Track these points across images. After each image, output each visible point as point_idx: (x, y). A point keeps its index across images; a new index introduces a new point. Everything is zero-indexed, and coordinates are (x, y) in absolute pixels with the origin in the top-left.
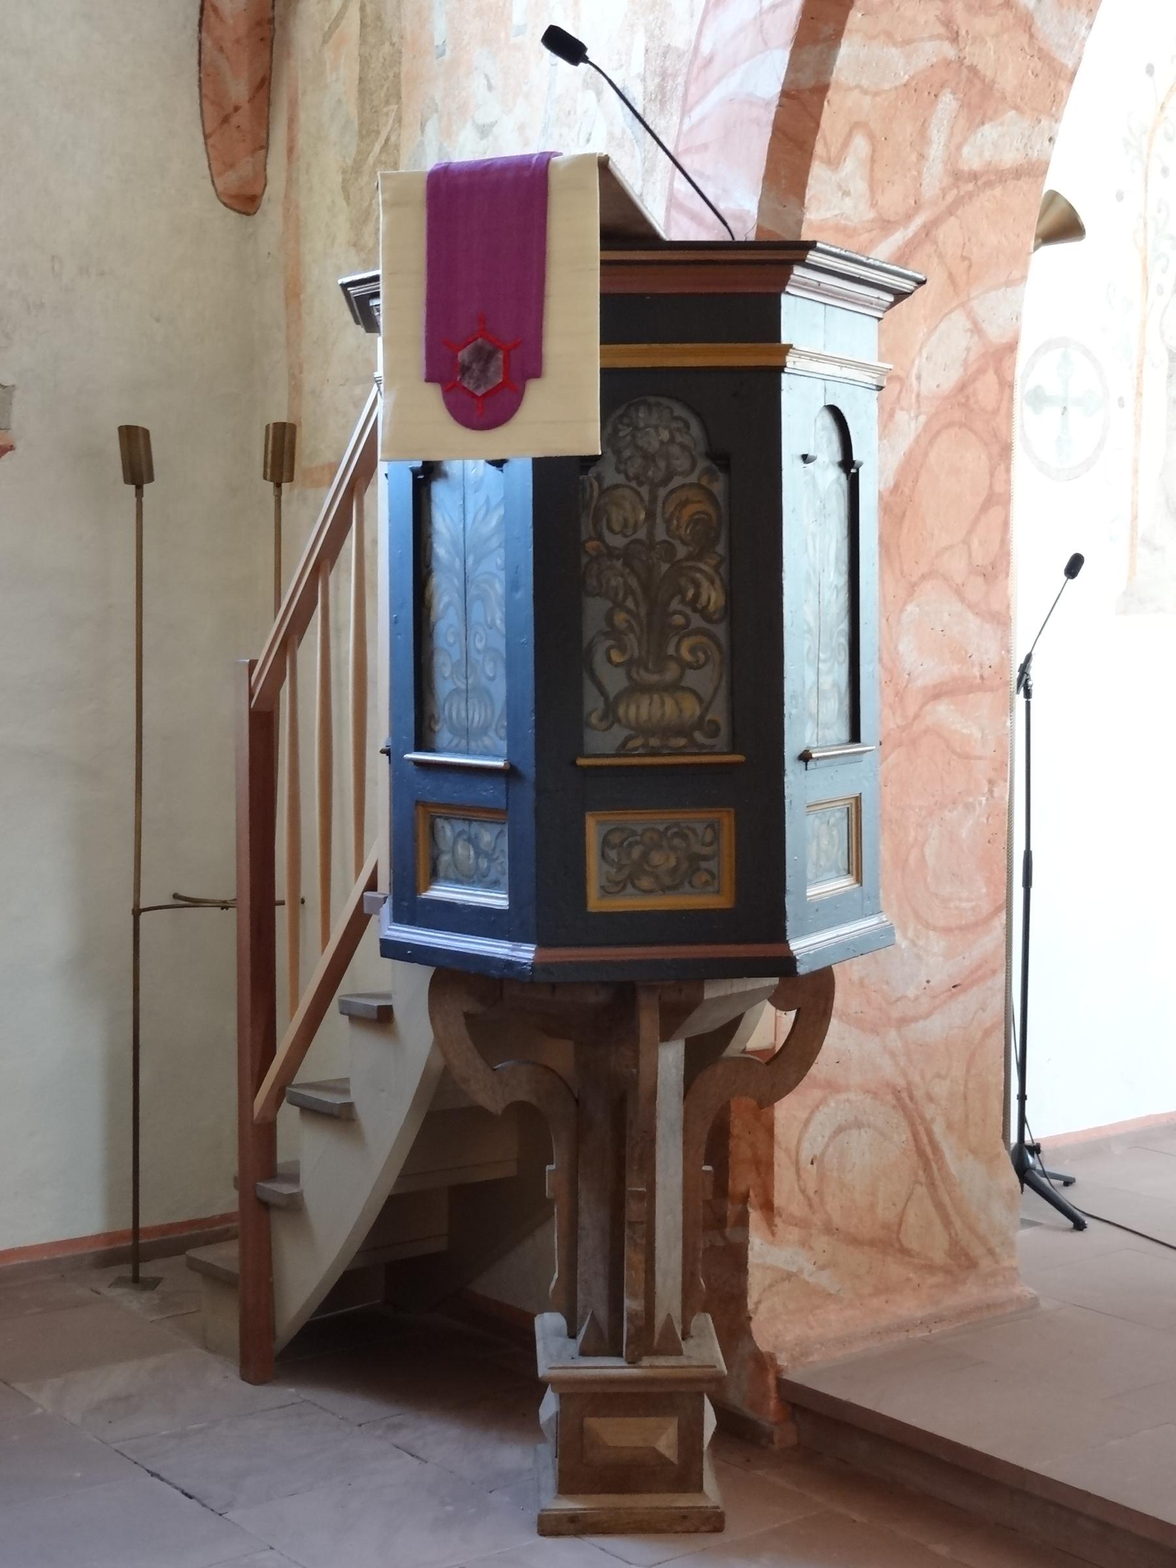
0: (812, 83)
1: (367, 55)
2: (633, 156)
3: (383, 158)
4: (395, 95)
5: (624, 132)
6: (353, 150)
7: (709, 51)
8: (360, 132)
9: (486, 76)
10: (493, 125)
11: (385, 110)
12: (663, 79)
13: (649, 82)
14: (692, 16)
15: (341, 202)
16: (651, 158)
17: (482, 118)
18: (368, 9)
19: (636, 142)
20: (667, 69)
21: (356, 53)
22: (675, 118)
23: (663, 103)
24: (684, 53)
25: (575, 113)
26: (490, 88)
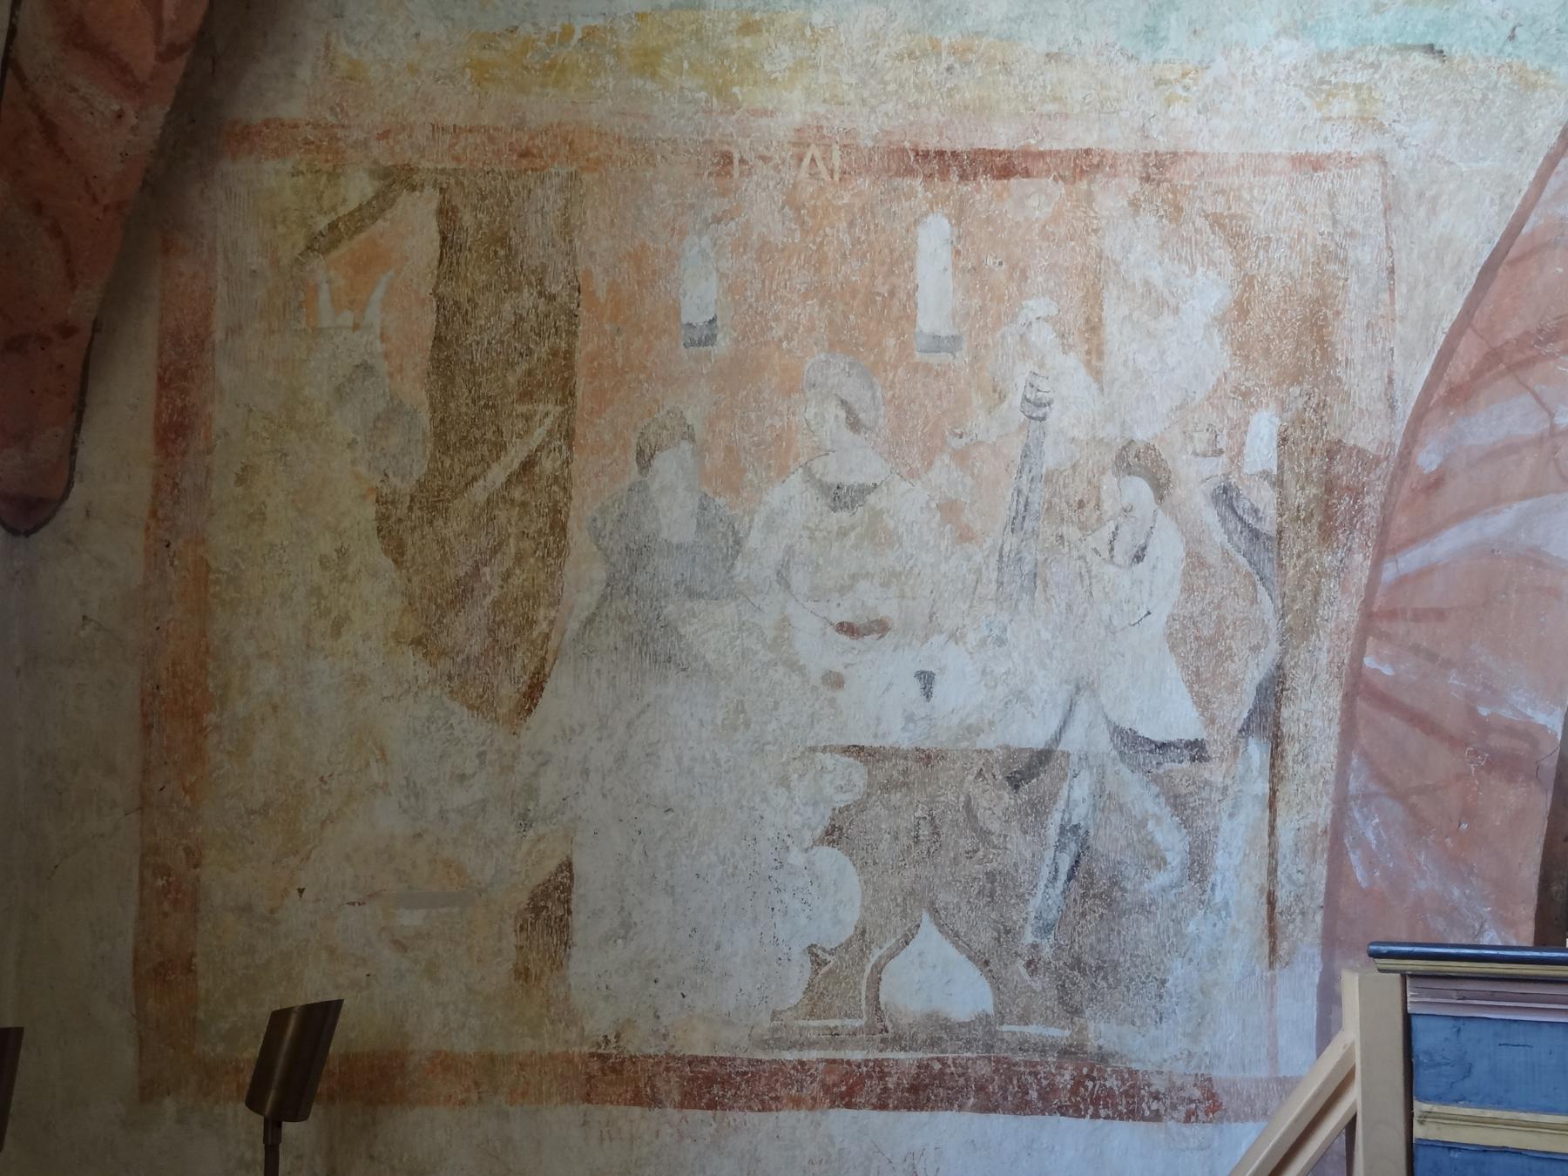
2: (1254, 601)
3: (517, 494)
5: (1227, 557)
7: (1434, 467)
8: (439, 436)
9: (843, 403)
10: (864, 490)
11: (521, 408)
13: (1292, 488)
14: (1392, 407)
17: (832, 471)
18: (467, 218)
19: (1261, 579)
20: (1339, 477)
21: (426, 291)
22: (1359, 557)
23: (1327, 533)
24: (1377, 461)
25: (1098, 506)
26: (854, 425)
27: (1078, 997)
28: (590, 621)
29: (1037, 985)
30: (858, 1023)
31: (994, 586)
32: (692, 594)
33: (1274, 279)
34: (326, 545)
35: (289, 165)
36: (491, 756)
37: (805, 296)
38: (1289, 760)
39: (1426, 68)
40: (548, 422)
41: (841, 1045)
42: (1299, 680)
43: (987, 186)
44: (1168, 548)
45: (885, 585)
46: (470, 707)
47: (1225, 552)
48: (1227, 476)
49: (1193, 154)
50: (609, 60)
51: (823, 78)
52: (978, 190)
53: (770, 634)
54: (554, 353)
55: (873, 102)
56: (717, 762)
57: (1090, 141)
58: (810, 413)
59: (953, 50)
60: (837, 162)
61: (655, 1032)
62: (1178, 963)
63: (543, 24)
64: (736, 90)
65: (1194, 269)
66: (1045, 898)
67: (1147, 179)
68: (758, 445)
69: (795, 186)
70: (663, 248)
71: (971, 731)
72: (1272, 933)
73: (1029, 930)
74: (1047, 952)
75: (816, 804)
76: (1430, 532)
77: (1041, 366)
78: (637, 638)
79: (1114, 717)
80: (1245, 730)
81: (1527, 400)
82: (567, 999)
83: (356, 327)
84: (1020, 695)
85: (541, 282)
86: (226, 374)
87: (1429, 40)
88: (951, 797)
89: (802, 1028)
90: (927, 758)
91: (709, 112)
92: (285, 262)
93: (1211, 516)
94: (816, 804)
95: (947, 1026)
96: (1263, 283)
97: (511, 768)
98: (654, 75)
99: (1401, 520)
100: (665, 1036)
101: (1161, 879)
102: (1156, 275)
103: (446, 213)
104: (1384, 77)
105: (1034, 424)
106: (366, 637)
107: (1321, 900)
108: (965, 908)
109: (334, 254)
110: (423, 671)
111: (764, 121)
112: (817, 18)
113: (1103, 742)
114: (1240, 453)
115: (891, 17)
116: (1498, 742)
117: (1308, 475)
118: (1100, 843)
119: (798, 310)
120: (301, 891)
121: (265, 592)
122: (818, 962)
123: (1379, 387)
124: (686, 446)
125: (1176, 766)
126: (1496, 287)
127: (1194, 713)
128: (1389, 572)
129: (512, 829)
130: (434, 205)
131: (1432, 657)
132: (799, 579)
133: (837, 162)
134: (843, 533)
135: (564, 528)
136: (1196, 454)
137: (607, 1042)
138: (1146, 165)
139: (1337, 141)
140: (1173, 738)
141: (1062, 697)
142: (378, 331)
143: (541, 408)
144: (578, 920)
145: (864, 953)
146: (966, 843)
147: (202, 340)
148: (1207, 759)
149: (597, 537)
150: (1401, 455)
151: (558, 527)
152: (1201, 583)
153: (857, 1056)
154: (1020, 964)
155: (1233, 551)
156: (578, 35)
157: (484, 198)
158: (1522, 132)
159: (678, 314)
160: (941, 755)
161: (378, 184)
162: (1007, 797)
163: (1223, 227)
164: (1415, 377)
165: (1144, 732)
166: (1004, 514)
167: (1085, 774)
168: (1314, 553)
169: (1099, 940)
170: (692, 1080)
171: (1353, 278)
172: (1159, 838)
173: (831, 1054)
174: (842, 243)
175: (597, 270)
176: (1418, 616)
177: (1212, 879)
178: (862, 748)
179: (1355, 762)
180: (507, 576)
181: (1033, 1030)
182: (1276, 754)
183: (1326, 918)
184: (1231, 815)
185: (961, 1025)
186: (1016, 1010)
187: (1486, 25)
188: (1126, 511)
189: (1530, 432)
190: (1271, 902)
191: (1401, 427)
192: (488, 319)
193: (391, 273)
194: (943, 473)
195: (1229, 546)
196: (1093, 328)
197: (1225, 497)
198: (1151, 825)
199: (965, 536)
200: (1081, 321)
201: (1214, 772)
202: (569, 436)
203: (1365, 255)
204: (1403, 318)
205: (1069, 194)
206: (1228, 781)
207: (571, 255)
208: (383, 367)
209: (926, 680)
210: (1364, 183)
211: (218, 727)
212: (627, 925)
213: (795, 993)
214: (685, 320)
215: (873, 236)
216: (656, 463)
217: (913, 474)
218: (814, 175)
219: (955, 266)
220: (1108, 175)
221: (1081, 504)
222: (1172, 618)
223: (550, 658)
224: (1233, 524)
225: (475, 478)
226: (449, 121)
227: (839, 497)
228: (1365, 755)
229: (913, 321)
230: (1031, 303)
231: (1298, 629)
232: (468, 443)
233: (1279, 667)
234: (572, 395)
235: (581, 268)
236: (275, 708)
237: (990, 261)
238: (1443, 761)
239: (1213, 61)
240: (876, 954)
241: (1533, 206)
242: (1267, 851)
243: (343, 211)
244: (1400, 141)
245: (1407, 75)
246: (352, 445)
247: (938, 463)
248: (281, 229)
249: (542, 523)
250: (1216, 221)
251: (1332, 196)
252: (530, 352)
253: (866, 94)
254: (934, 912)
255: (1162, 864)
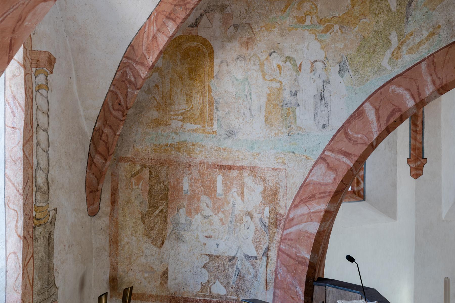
0: (323, 230)
1: (153, 185)
2: (265, 236)
3: (160, 214)
4: (166, 198)
6: (146, 209)
7: (292, 217)
8: (149, 205)
10: (209, 216)
11: (161, 202)
12: (276, 220)
13: (271, 219)
14: (286, 207)
15: (140, 222)
16: (272, 238)
17: (205, 213)
18: (153, 173)
20: (278, 218)
21: (147, 183)
22: (280, 230)
23: (276, 226)
25: (243, 220)
26: (208, 207)
27: (238, 293)
28: (170, 234)
29: (233, 291)
30: (208, 294)
31: (227, 232)
32: (185, 230)
33: (269, 187)
34: (134, 221)
35: (129, 164)
36: (157, 252)
37: (201, 187)
38: (269, 260)
39: (292, 156)
40: (165, 204)
41: (205, 297)
42: (271, 248)
43: (227, 170)
44: (253, 228)
45: (212, 231)
46: (154, 245)
47: (261, 228)
48: (261, 217)
49: (258, 167)
50: (173, 149)
51: (204, 153)
52: (226, 171)
53: (196, 237)
54: (165, 194)
55: (211, 157)
56: (188, 255)
57: (243, 164)
58: (201, 204)
59: (223, 149)
60: (206, 167)
61: (180, 293)
62: (253, 289)
63: (164, 143)
64: (191, 154)
65: (257, 185)
66: (234, 278)
67: (251, 171)
68: (194, 209)
69: (199, 170)
70: (181, 179)
71: (224, 253)
72: (266, 285)
73: (232, 283)
74: (234, 286)
75: (202, 262)
76: (291, 227)
77: (235, 199)
78: (177, 236)
79: (244, 252)
80: (263, 255)
81: (306, 207)
82: (167, 288)
83: (138, 188)
84: (230, 248)
85: (164, 183)
86: (120, 194)
87: (293, 151)
88: (221, 262)
89: (200, 294)
90: (218, 256)
91: (187, 158)
92: (128, 178)
93: (259, 223)
94: (202, 262)
95: (220, 295)
96: (267, 188)
97: (160, 254)
98: (180, 151)
99: (287, 225)
100: (181, 294)
101: (250, 276)
102: (252, 186)
103: (150, 172)
104: (286, 156)
105: (234, 208)
106: (140, 234)
107: (274, 281)
108: (223, 279)
109: (135, 177)
110: (147, 240)
111: (195, 159)
112: (203, 144)
113: (243, 256)
114: (263, 213)
115: (214, 144)
116: (300, 259)
117: (273, 217)
118: (242, 271)
119: (200, 189)
120: (131, 270)
121: (126, 227)
122: (202, 285)
123: (284, 204)
124: (184, 208)
125: (253, 260)
126: (302, 190)
127: (256, 252)
128: (285, 233)
129: (160, 263)
130: (149, 171)
131: (291, 246)
132: (200, 229)
133: (206, 167)
134: (206, 223)
135: (167, 220)
136: (257, 213)
137: (173, 294)
138: (251, 168)
139: (279, 166)
140: (253, 256)
141: (236, 249)
142: (141, 189)
143: (164, 202)
144: (169, 277)
145: (208, 284)
146: (223, 269)
147: (117, 189)
148: (258, 259)
149: (171, 221)
150: (287, 215)
151: (166, 220)
152: (257, 233)
153: (208, 299)
154: (230, 287)
155: (262, 228)
156: (169, 145)
157: (156, 170)
158: (306, 166)
159: (183, 189)
160: (220, 256)
161: (141, 167)
162: (229, 263)
163: (262, 178)
164: (290, 203)
165: (248, 255)
166: (229, 221)
167: (240, 260)
168: (274, 229)
169: (241, 285)
170: (185, 301)
171: (281, 187)
172: (250, 270)
173: (204, 298)
174: (206, 179)
175: (171, 182)
176: (289, 240)
177: (258, 277)
178: (208, 254)
179: (279, 261)
180: (159, 226)
181: (232, 297)
182: (267, 259)
183: (274, 284)
184: (261, 268)
185: (222, 296)
186: (230, 294)
187: (301, 149)
188: (247, 221)
189: (307, 212)
190: (266, 281)
191: (287, 211)
192: (156, 188)
193: (143, 181)
194: (220, 215)
195: (261, 227)
196: (243, 193)
197: (261, 220)
198: (249, 268)
199: (223, 224)
200: (241, 192)
201: (258, 261)
202: (168, 206)
203: (282, 184)
204: (288, 194)
205: (239, 172)
206: (260, 263)
207: (168, 179)
208: (142, 194)
209: (218, 245)
210: (283, 173)
211: (120, 246)
212: (176, 278)
213: (199, 289)
214: (184, 189)
215: (211, 178)
216: (180, 211)
217: (216, 214)
218: (202, 168)
219: (222, 183)
220: (245, 170)
221: (240, 220)
222: (253, 238)
223: (165, 238)
224: (262, 224)
225: (154, 212)
226: (151, 158)
227: (205, 217)
228: (280, 260)
229: (216, 191)
230: (234, 189)
231: (271, 241)
232: (153, 207)
233: (268, 246)
234: (168, 200)
235: (169, 181)
236: (128, 243)
237: (228, 182)
238: (292, 262)
239: (261, 152)
240: (210, 284)
241: (308, 177)
242: (266, 273)
243: (136, 171)
244: (288, 166)
245: (289, 156)
246: (137, 206)
247: (220, 213)
248: (127, 173)
249: (164, 219)
250: (261, 177)
251: (278, 174)
252: (162, 193)
253: (210, 156)
254: (218, 279)
255: (251, 274)
